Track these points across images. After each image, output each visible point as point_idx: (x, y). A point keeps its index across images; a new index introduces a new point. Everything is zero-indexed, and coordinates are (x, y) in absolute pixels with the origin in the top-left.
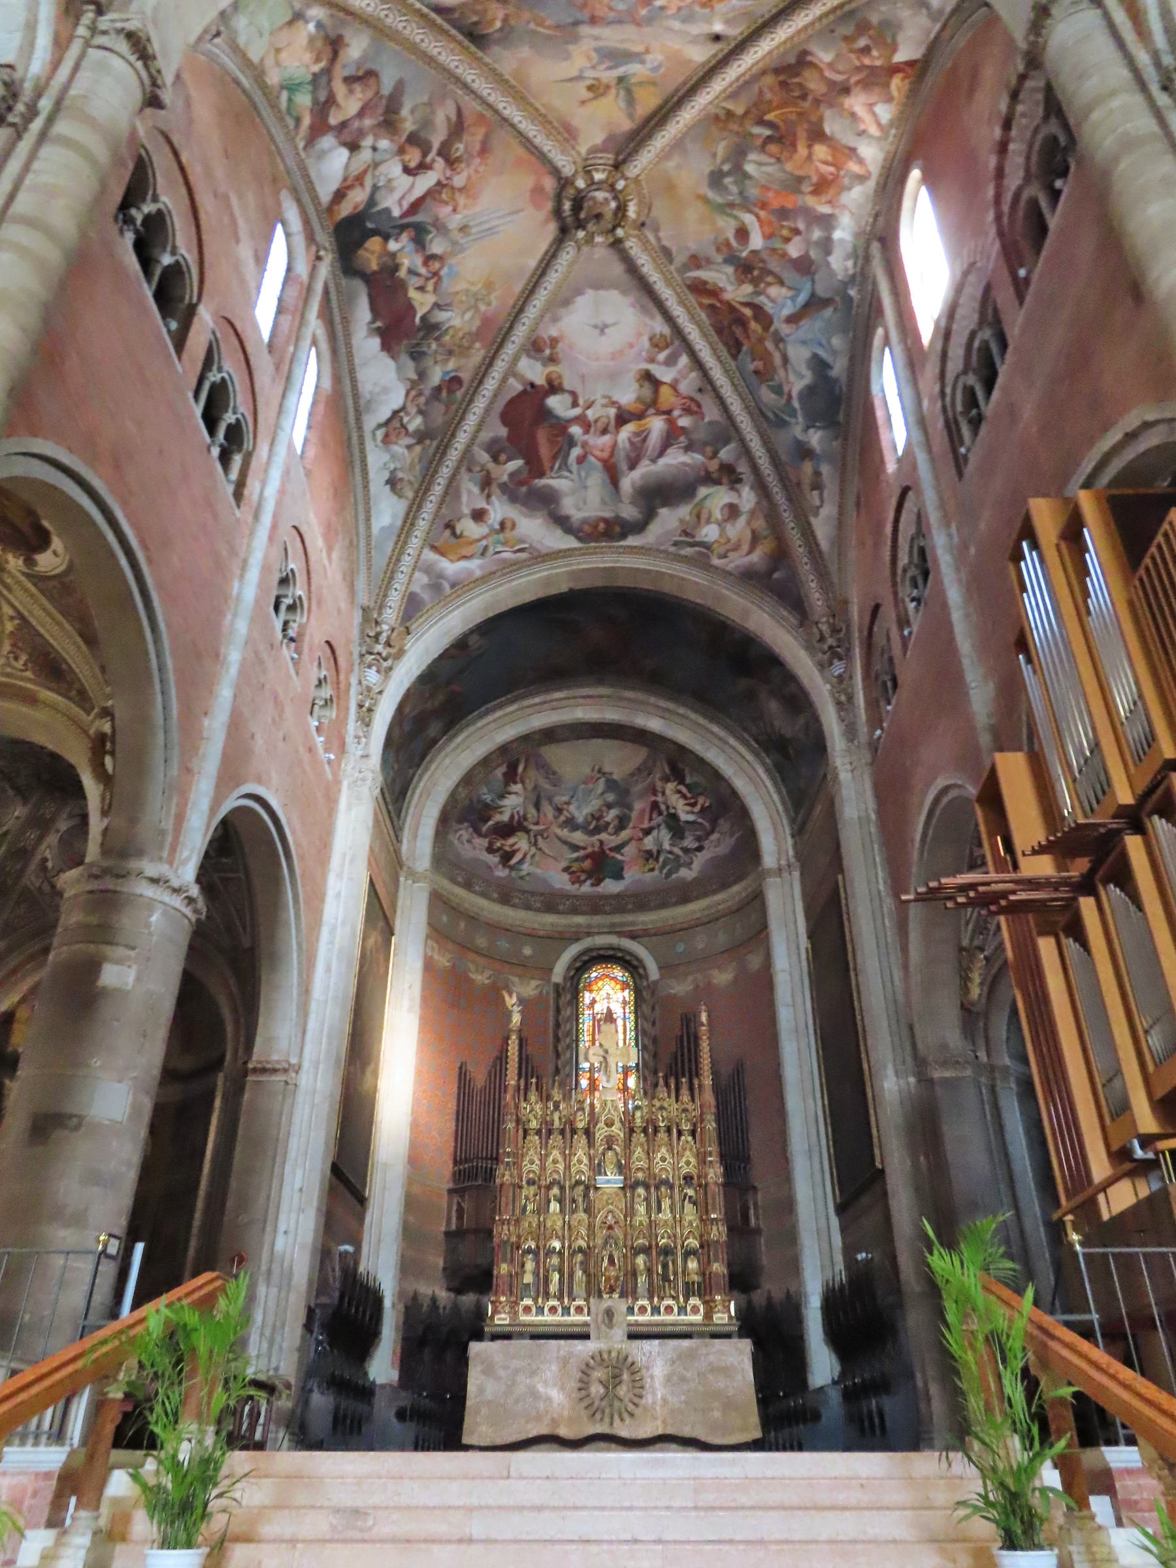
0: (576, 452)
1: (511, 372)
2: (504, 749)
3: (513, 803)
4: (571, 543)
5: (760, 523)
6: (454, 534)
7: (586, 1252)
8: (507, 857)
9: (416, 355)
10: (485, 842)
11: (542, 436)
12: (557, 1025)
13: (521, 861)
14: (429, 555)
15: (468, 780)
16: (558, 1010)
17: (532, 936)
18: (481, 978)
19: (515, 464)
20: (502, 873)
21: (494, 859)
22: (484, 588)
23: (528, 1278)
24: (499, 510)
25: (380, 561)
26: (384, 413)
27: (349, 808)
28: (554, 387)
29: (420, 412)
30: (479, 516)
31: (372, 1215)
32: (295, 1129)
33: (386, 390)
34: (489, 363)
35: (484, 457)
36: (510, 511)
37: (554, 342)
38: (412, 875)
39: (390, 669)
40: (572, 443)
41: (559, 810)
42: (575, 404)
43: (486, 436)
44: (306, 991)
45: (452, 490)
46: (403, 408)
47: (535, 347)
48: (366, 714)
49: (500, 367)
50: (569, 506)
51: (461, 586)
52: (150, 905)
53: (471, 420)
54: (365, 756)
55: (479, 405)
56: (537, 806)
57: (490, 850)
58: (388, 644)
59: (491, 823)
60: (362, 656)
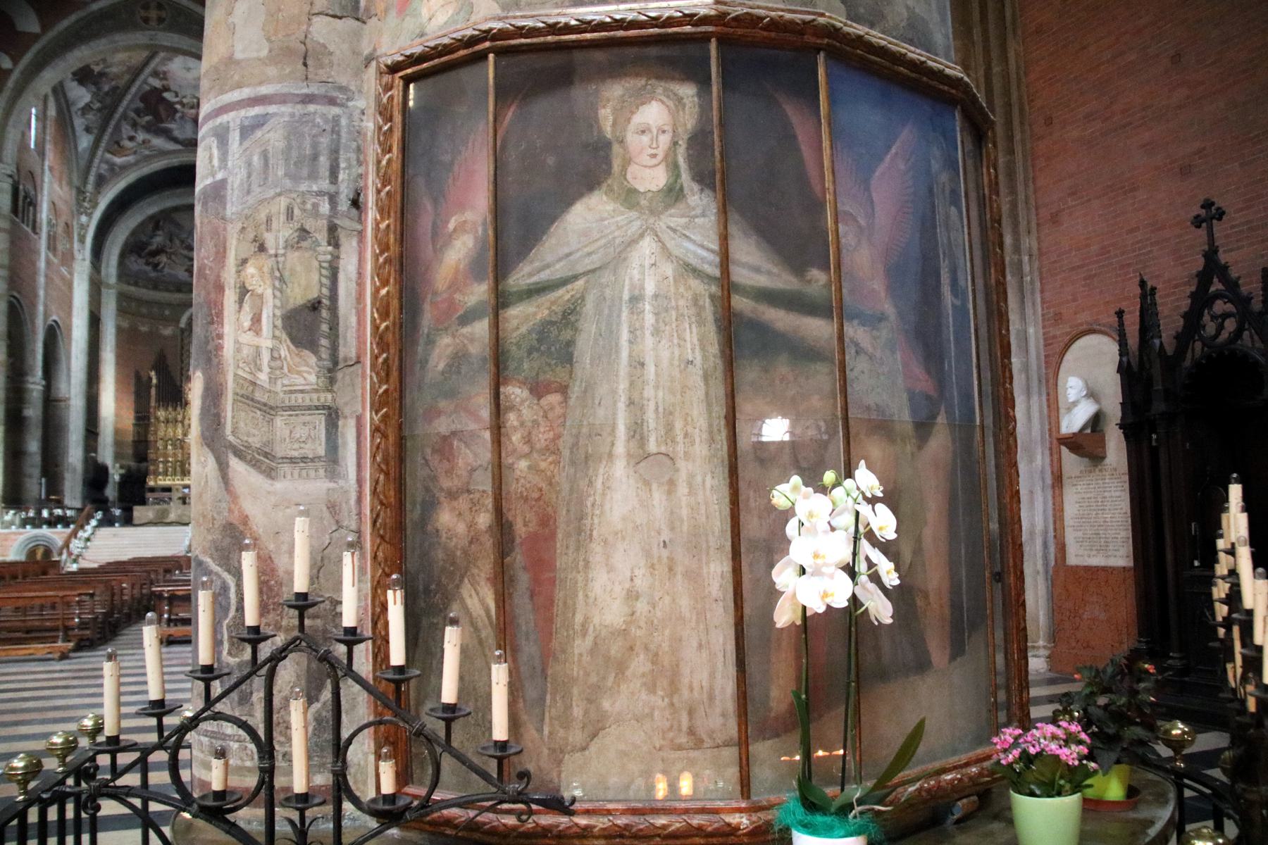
0: (178, 115)
1: (145, 82)
2: (151, 218)
3: (159, 240)
4: (179, 147)
6: (119, 145)
7: (181, 462)
8: (155, 266)
9: (96, 84)
10: (144, 261)
11: (162, 109)
12: (182, 348)
13: (163, 267)
14: (108, 156)
15: (134, 233)
16: (182, 340)
17: (170, 305)
18: (144, 329)
19: (148, 118)
20: (153, 274)
21: (148, 268)
22: (135, 168)
23: (161, 470)
24: (141, 136)
25: (83, 163)
26: (81, 104)
27: (79, 285)
28: (166, 89)
29: (99, 101)
30: (131, 139)
31: (101, 439)
32: (71, 420)
33: (82, 97)
34: (133, 81)
35: (132, 115)
36: (148, 136)
37: (165, 73)
38: (108, 286)
39: (91, 213)
40: (176, 111)
41: (182, 242)
42: (177, 96)
43: (133, 106)
44: (69, 369)
45: (117, 128)
46: (91, 102)
47: (155, 74)
48: (82, 240)
49: (138, 83)
50: (177, 133)
51: (124, 168)
52: (32, 390)
53: (125, 103)
54: (84, 260)
55: (128, 97)
56: (171, 240)
57: (148, 264)
58: (90, 201)
59: (146, 251)
60: (78, 210)
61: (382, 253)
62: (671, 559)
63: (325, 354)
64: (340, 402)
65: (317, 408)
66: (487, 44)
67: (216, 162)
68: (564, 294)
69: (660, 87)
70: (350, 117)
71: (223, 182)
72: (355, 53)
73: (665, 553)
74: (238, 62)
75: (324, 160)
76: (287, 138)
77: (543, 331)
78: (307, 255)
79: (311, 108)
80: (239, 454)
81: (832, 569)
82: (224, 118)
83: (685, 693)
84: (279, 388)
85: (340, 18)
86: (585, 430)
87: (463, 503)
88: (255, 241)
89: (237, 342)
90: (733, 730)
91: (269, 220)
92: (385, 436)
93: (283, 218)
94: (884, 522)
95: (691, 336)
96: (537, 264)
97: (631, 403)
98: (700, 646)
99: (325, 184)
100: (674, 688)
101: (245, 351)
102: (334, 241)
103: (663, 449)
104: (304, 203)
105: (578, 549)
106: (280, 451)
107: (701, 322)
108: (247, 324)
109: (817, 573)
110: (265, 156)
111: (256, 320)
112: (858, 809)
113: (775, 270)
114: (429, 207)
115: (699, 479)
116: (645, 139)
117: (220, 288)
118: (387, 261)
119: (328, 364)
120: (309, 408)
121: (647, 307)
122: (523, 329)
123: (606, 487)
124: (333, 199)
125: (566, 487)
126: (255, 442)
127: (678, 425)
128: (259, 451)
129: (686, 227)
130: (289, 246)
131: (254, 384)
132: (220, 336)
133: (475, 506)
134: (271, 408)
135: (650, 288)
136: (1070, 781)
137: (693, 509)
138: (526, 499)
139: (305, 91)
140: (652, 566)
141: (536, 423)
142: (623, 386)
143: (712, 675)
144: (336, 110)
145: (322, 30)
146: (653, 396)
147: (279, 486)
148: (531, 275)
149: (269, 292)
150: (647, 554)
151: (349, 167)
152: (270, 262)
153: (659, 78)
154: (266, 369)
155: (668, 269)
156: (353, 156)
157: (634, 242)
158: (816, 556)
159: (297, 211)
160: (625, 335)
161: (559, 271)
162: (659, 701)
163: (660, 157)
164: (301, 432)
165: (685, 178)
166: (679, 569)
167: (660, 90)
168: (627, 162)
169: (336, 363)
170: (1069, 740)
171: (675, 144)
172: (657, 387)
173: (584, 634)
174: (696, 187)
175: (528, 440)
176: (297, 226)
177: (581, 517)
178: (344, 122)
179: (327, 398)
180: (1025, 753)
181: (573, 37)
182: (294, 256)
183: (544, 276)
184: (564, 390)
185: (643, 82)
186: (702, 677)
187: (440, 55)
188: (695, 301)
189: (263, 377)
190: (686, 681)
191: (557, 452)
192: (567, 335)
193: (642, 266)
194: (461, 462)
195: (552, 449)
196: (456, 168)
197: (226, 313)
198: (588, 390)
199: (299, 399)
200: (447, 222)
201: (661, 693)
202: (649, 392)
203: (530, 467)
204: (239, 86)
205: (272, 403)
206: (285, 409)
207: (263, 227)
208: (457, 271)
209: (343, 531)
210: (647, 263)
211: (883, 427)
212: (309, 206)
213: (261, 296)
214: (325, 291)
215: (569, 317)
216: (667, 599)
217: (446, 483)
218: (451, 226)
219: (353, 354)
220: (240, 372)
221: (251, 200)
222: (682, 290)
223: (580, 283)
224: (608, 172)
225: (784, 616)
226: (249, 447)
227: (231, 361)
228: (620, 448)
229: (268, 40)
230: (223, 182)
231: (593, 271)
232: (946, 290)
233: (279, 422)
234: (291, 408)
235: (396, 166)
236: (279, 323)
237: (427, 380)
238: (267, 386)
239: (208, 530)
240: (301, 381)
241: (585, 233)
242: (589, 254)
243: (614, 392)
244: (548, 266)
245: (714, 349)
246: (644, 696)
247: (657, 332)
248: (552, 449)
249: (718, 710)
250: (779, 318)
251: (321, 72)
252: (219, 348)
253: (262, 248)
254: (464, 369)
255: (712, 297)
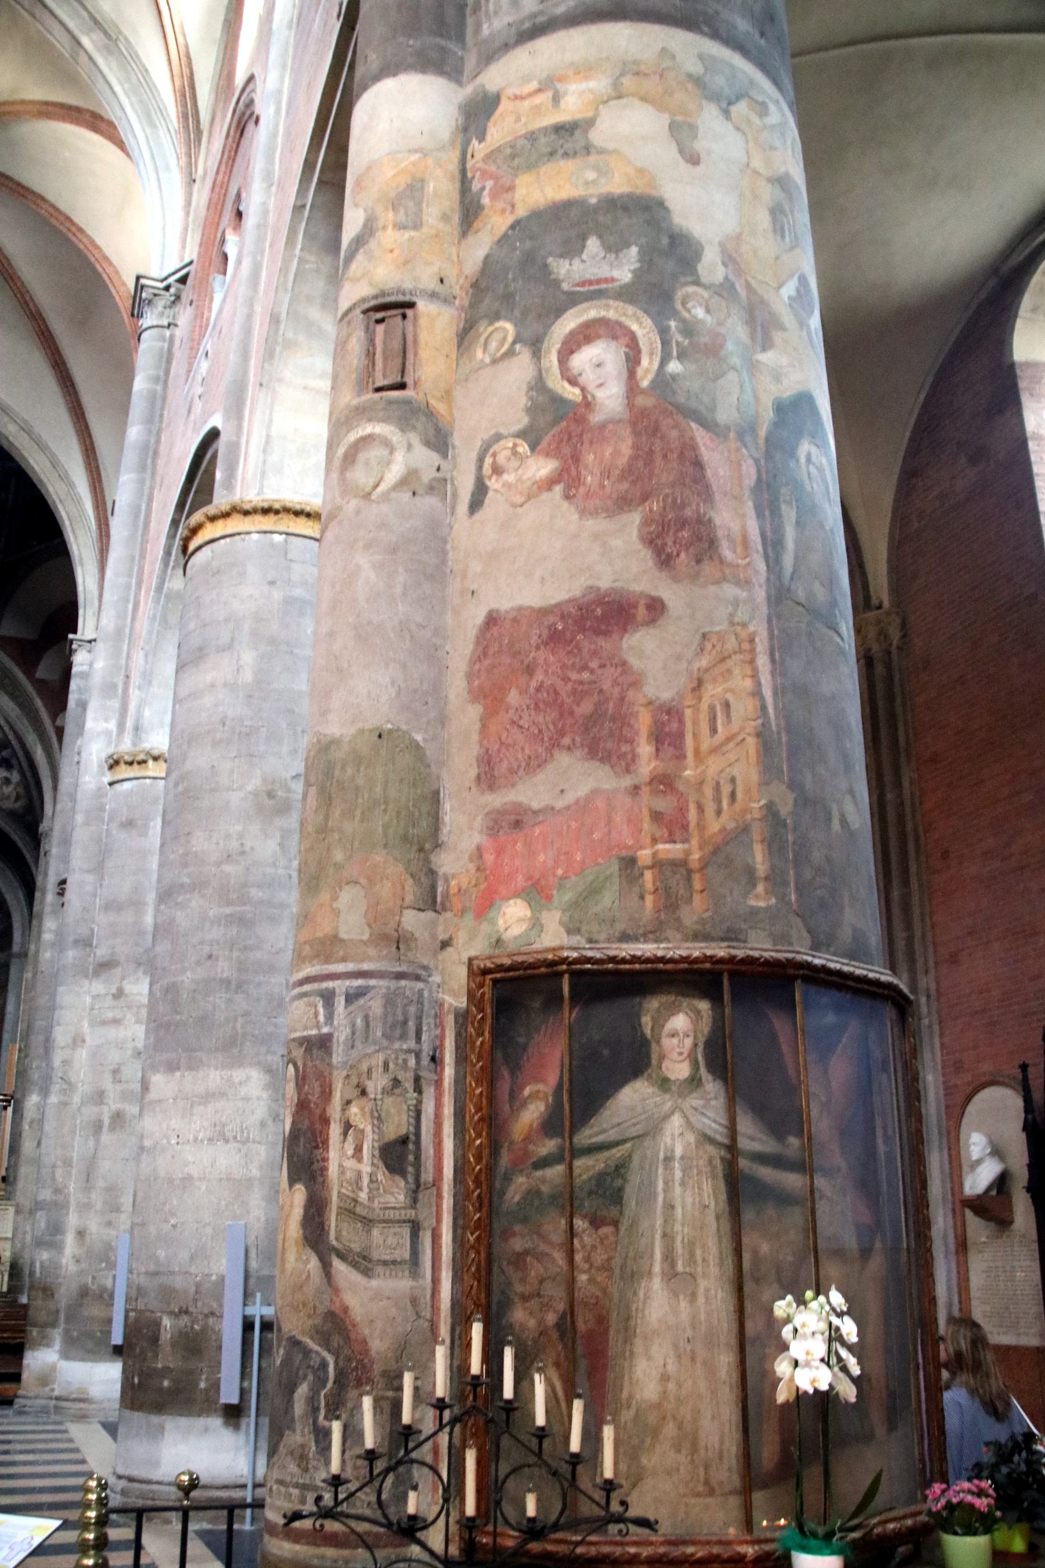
5: (21, 790)
61: (476, 1113)
62: (693, 1352)
63: (411, 1179)
64: (421, 1217)
65: (404, 1222)
66: (564, 967)
67: (321, 1018)
68: (617, 1153)
69: (685, 1002)
70: (430, 992)
71: (328, 1037)
72: (434, 937)
73: (688, 1348)
74: (342, 941)
75: (411, 1024)
76: (385, 1007)
77: (601, 1177)
78: (399, 1099)
79: (403, 983)
80: (342, 1257)
81: (817, 1363)
82: (330, 984)
83: (702, 1452)
84: (376, 1205)
85: (423, 911)
86: (631, 1254)
87: (534, 1303)
88: (358, 1086)
89: (340, 1166)
90: (736, 1482)
91: (369, 1071)
92: (478, 1252)
93: (381, 1070)
94: (849, 1329)
95: (707, 1187)
96: (595, 1129)
97: (665, 1235)
98: (713, 1417)
99: (411, 1044)
100: (694, 1448)
101: (349, 1175)
102: (418, 1089)
103: (687, 1270)
104: (397, 1058)
105: (625, 1342)
106: (375, 1255)
107: (714, 1177)
108: (350, 1152)
109: (808, 1364)
110: (366, 1018)
111: (359, 1150)
112: (838, 1535)
113: (764, 1138)
114: (506, 1074)
115: (713, 1292)
116: (675, 1041)
117: (326, 1121)
118: (482, 1119)
119: (413, 1186)
120: (399, 1222)
121: (677, 1165)
122: (585, 1177)
123: (647, 1297)
124: (418, 1055)
125: (616, 1296)
126: (356, 1247)
127: (698, 1252)
128: (359, 1254)
129: (704, 1106)
130: (388, 1092)
131: (355, 1201)
132: (325, 1160)
133: (545, 1307)
134: (370, 1221)
135: (678, 1152)
136: (982, 1524)
137: (709, 1314)
138: (586, 1304)
139: (399, 969)
140: (679, 1356)
141: (594, 1247)
142: (659, 1222)
143: (722, 1443)
144: (420, 985)
145: (412, 920)
146: (681, 1231)
147: (374, 1283)
148: (591, 1137)
149: (369, 1129)
150: (676, 1346)
151: (429, 1030)
152: (371, 1104)
153: (684, 995)
154: (366, 1189)
155: (691, 1138)
156: (432, 1021)
157: (667, 1117)
158: (808, 1353)
159: (391, 1065)
160: (660, 1185)
161: (612, 1135)
162: (683, 1458)
163: (685, 1055)
164: (392, 1241)
165: (703, 1071)
166: (699, 1360)
167: (685, 1004)
168: (662, 1057)
169: (418, 1186)
170: (980, 1493)
171: (696, 1045)
172: (683, 1225)
173: (629, 1407)
174: (710, 1078)
175: (587, 1259)
176: (392, 1076)
177: (628, 1318)
178: (426, 994)
179: (411, 1214)
180: (949, 1502)
181: (627, 966)
182: (389, 1100)
183: (600, 1138)
184: (616, 1223)
185: (673, 998)
186: (714, 1440)
187: (526, 969)
188: (710, 1161)
189: (363, 1196)
190: (702, 1443)
191: (610, 1270)
192: (619, 1182)
193: (673, 1135)
194: (533, 1273)
195: (606, 1267)
196: (530, 1050)
197: (331, 1142)
198: (634, 1224)
199: (391, 1214)
200: (522, 1089)
201: (684, 1452)
202: (678, 1228)
203: (590, 1280)
204: (344, 960)
205: (370, 1216)
206: (379, 1222)
207: (365, 1076)
208: (531, 1126)
209: (421, 1321)
210: (677, 1132)
211: (839, 1253)
212: (400, 1061)
213: (363, 1131)
214: (412, 1129)
215: (620, 1169)
216: (690, 1382)
217: (519, 1288)
218: (527, 1092)
219: (431, 1179)
220: (344, 1191)
221: (355, 1053)
222: (701, 1152)
223: (628, 1145)
224: (648, 1064)
225: (782, 1396)
226: (350, 1250)
227: (336, 1181)
228: (657, 1268)
229: (369, 926)
230: (328, 1037)
231: (638, 1137)
232: (880, 1141)
233: (375, 1232)
234: (385, 1221)
235: (487, 1047)
236: (377, 1153)
237: (505, 1206)
238: (366, 1202)
239: (309, 1316)
240: (393, 1200)
241: (632, 1109)
242: (634, 1125)
243: (652, 1227)
244: (604, 1131)
245: (723, 1197)
246: (672, 1454)
247: (683, 1184)
248: (606, 1267)
249: (726, 1467)
250: (767, 1173)
251: (409, 954)
252: (324, 1169)
253: (364, 1093)
254: (536, 1203)
255: (722, 1159)
